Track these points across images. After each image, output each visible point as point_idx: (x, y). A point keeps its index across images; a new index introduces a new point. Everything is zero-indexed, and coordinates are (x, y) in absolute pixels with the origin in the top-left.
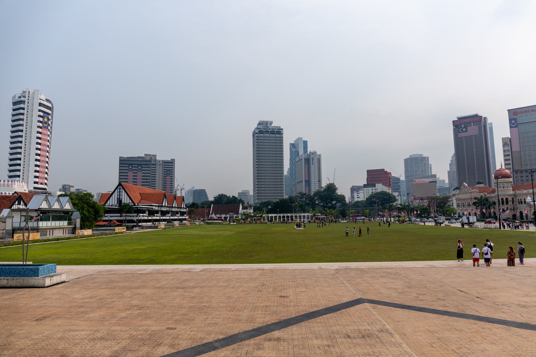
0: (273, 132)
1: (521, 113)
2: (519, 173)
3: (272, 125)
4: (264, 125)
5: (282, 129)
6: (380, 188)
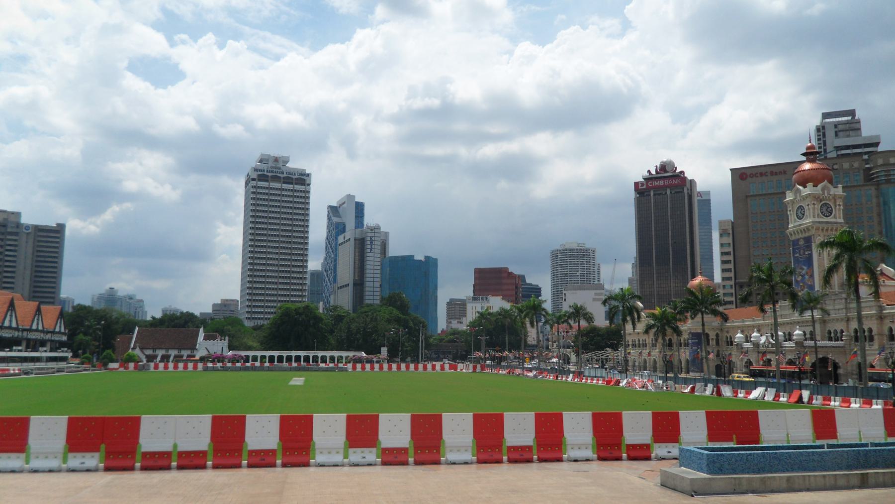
0: (288, 180)
1: (752, 176)
4: (271, 164)
5: (308, 175)
6: (497, 304)
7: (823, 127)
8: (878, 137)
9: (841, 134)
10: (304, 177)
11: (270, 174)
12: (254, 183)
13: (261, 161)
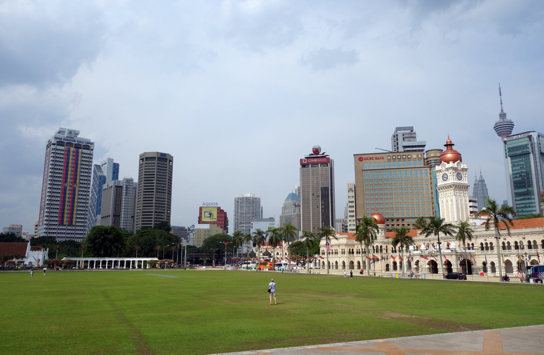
3: (78, 136)
4: (66, 135)
5: (92, 144)
7: (397, 135)
8: (425, 142)
10: (89, 145)
11: (66, 142)
12: (53, 147)
13: (59, 132)
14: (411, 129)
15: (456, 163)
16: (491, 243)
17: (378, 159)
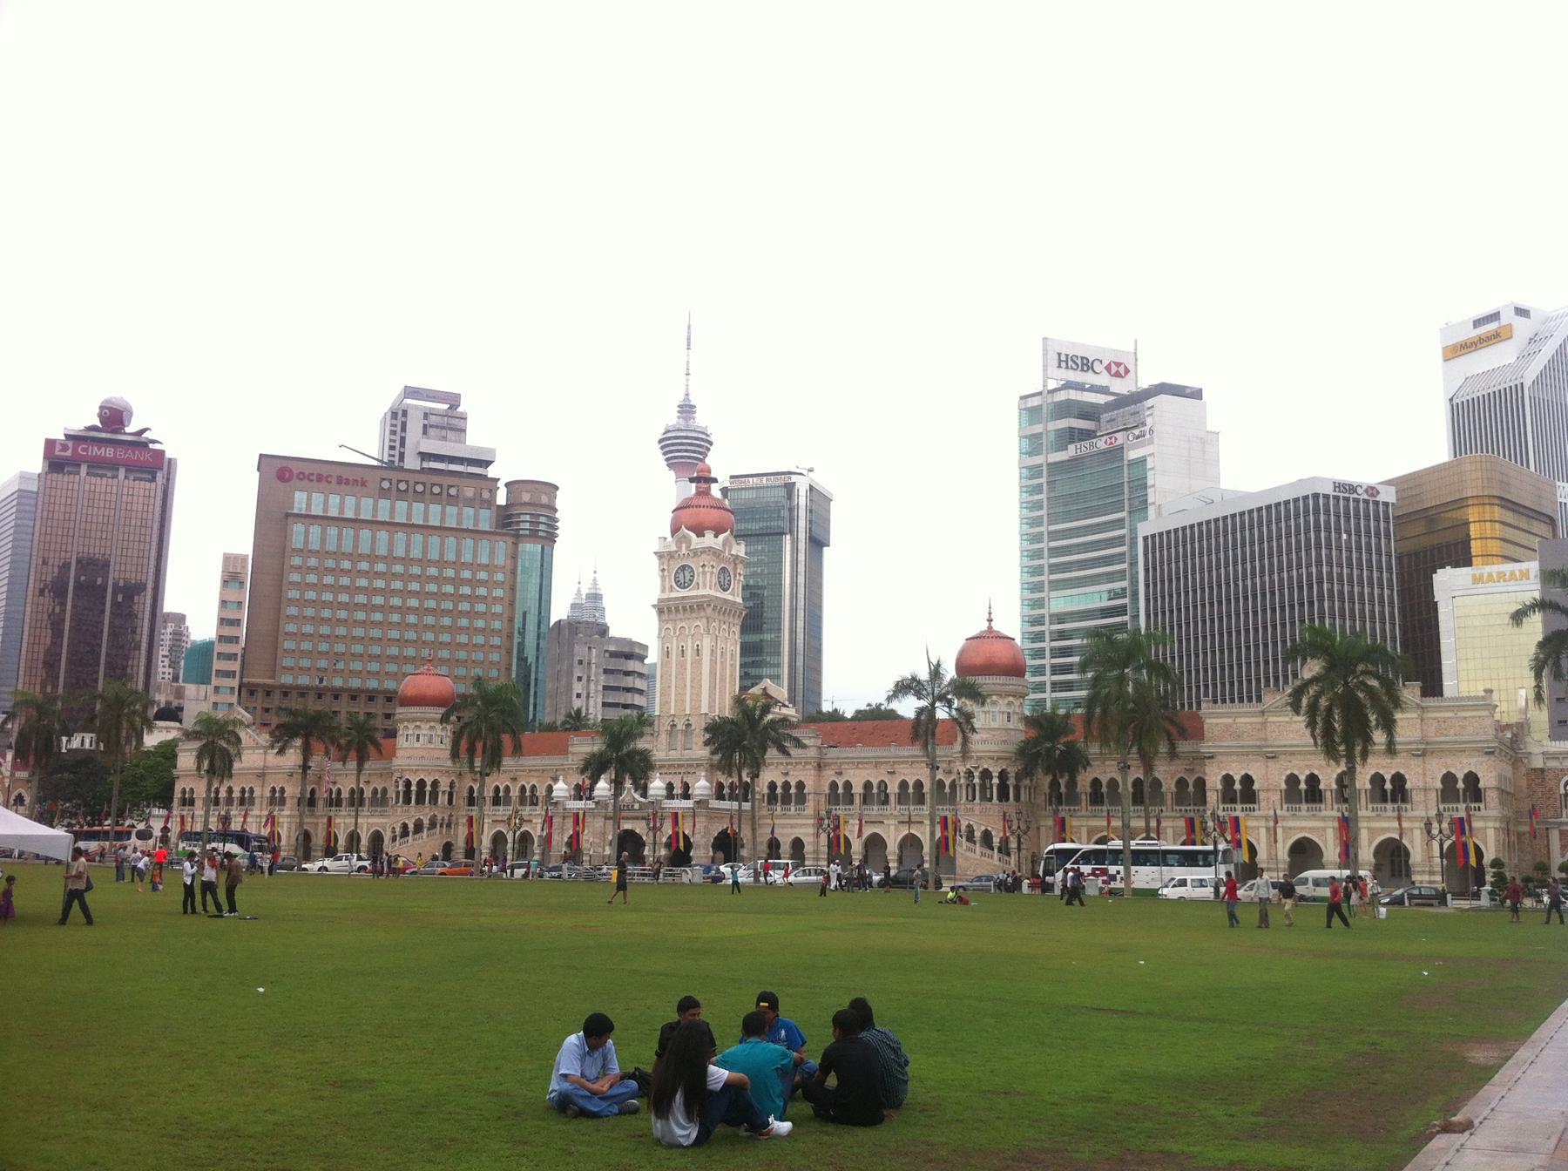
1: (302, 476)
2: (260, 695)
7: (405, 413)
8: (493, 451)
9: (432, 432)
14: (453, 400)
15: (722, 537)
16: (801, 785)
17: (347, 482)
